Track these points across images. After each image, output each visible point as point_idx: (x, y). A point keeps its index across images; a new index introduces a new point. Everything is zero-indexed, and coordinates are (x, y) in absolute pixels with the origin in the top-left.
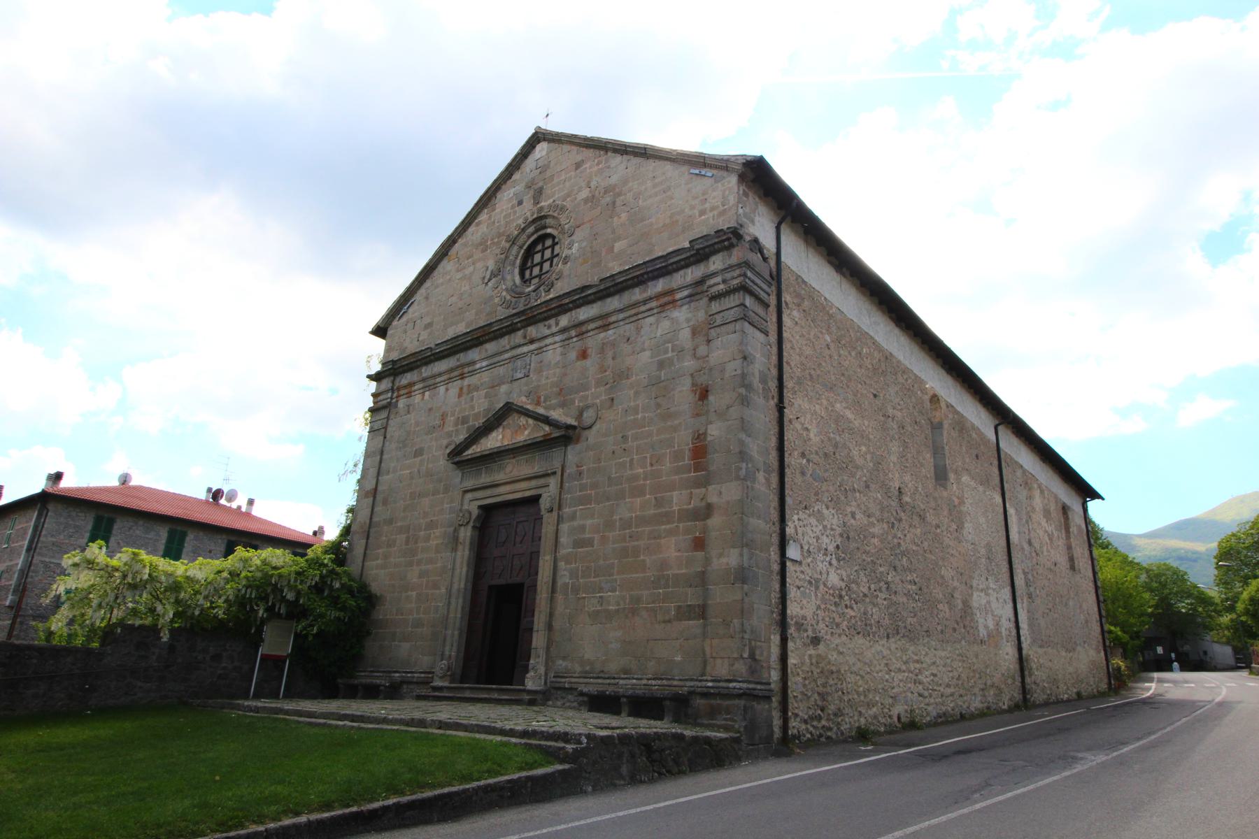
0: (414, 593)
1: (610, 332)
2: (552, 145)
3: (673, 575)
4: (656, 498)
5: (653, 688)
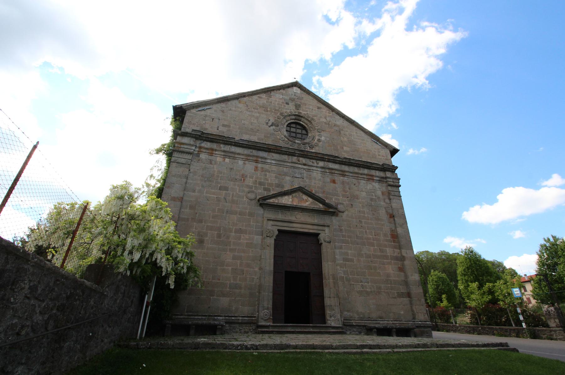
0: (230, 268)
1: (346, 178)
2: (302, 92)
3: (393, 280)
4: (379, 249)
5: (397, 324)
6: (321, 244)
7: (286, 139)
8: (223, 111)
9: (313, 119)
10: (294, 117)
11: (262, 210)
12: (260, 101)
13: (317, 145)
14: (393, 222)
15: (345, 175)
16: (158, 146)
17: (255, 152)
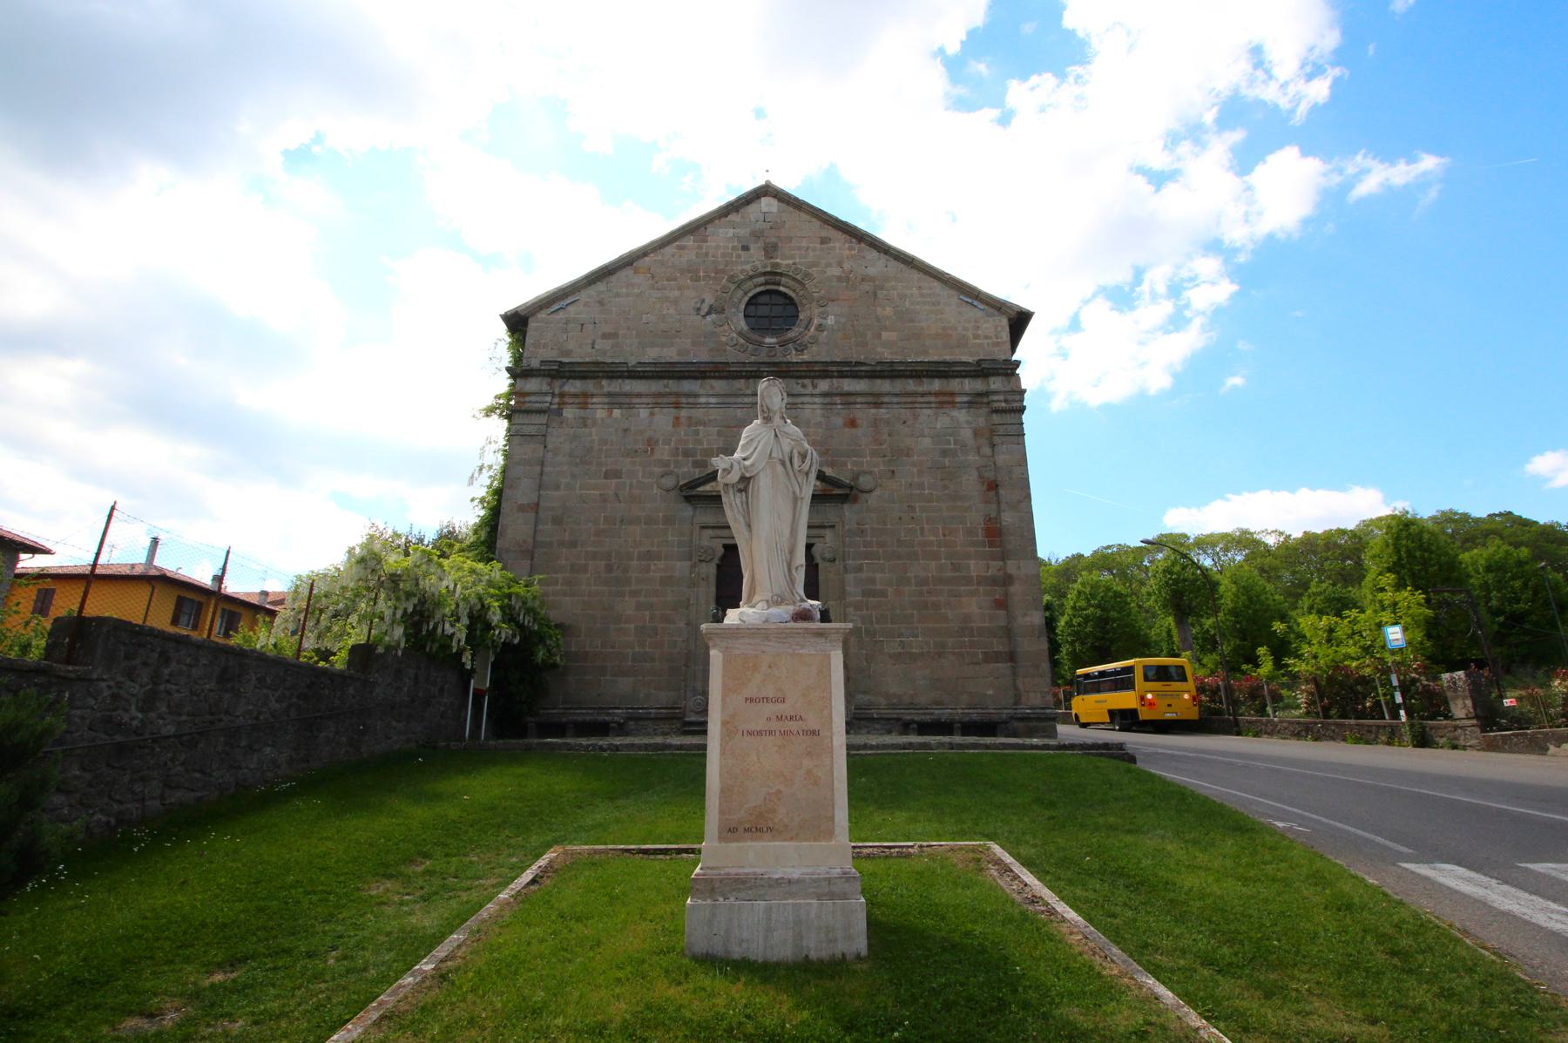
0: (632, 626)
1: (883, 411)
6: (817, 565)
7: (742, 341)
8: (601, 303)
9: (807, 275)
10: (762, 279)
11: (690, 508)
12: (681, 256)
13: (815, 341)
14: (995, 498)
15: (882, 403)
16: (489, 401)
17: (673, 385)
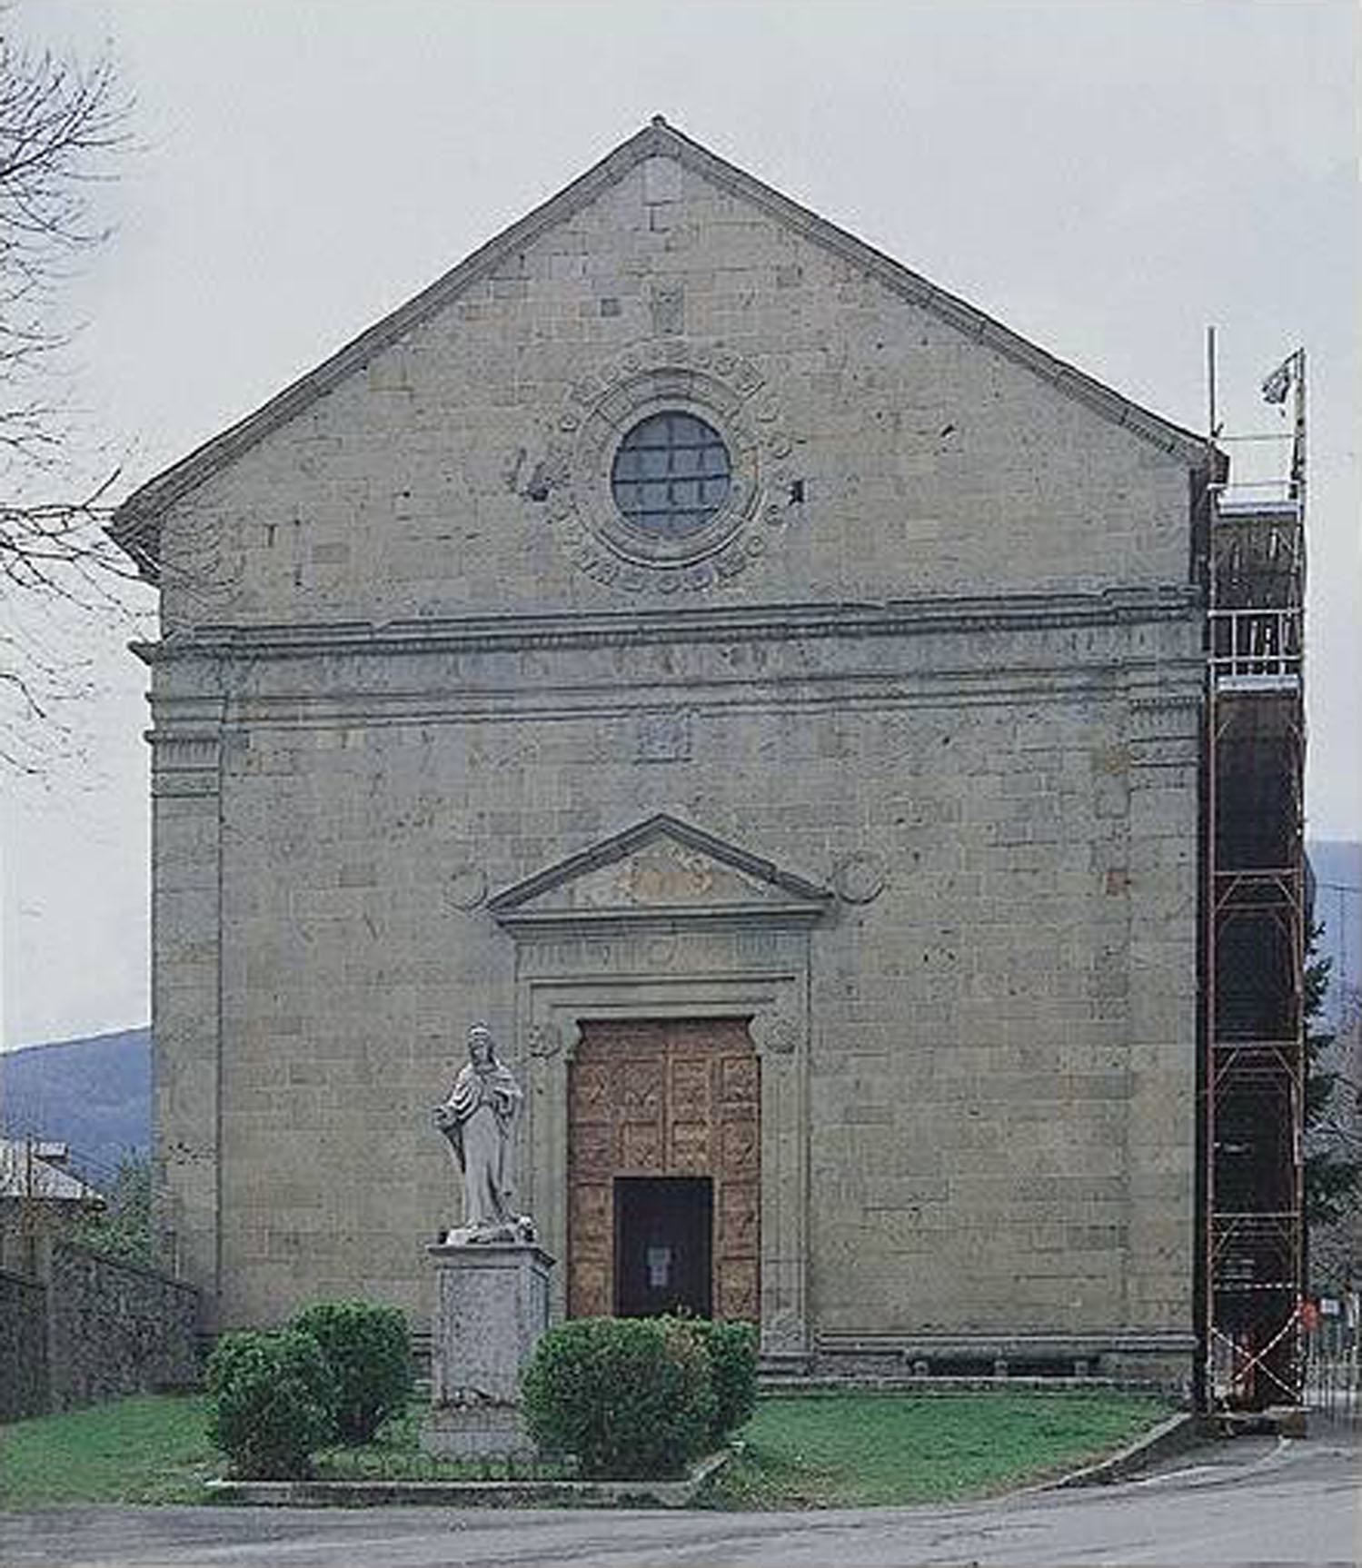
10: (647, 389)
17: (466, 669)
